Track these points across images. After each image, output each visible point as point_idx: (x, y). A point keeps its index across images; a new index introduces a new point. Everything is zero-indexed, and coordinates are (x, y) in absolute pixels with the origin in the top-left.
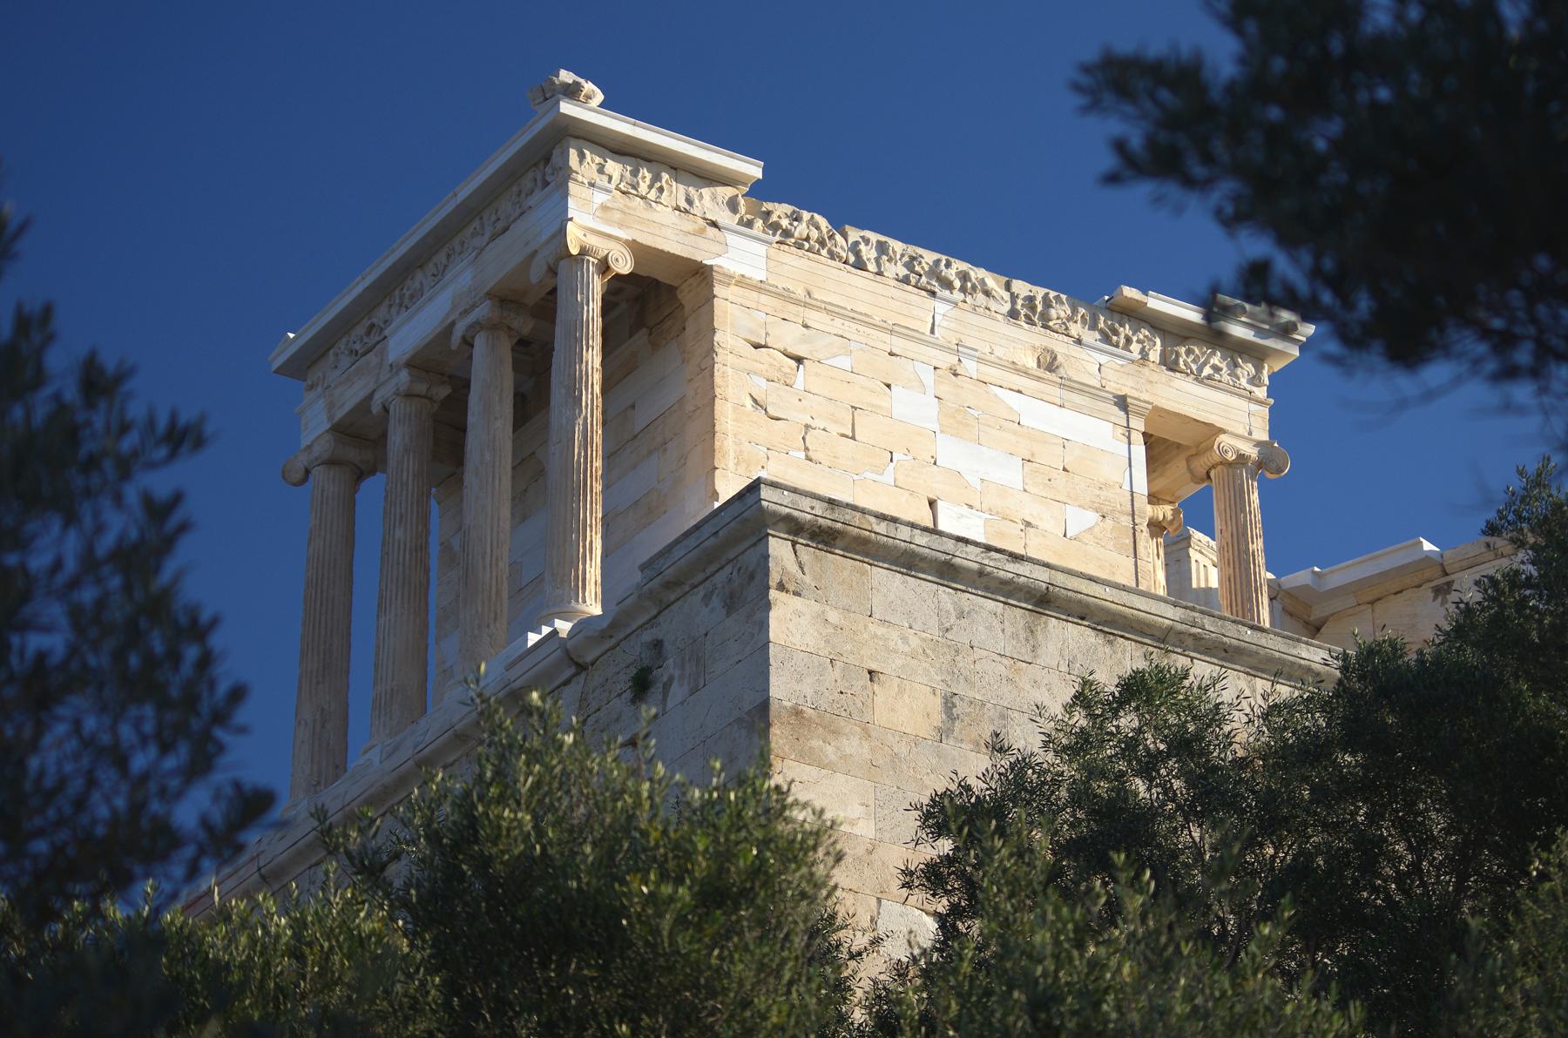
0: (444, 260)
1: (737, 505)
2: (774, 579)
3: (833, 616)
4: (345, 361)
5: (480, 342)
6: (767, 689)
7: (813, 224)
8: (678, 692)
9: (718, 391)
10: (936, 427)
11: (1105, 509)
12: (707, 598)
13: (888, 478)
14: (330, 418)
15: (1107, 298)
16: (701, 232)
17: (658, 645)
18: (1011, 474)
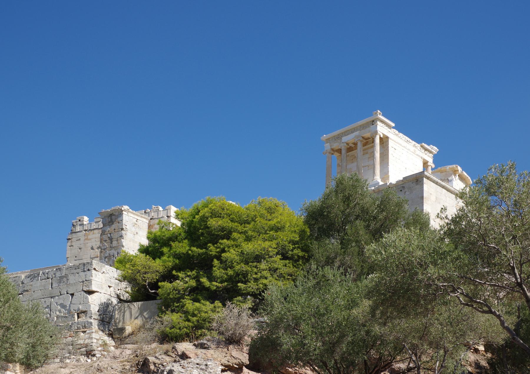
7: (397, 132)
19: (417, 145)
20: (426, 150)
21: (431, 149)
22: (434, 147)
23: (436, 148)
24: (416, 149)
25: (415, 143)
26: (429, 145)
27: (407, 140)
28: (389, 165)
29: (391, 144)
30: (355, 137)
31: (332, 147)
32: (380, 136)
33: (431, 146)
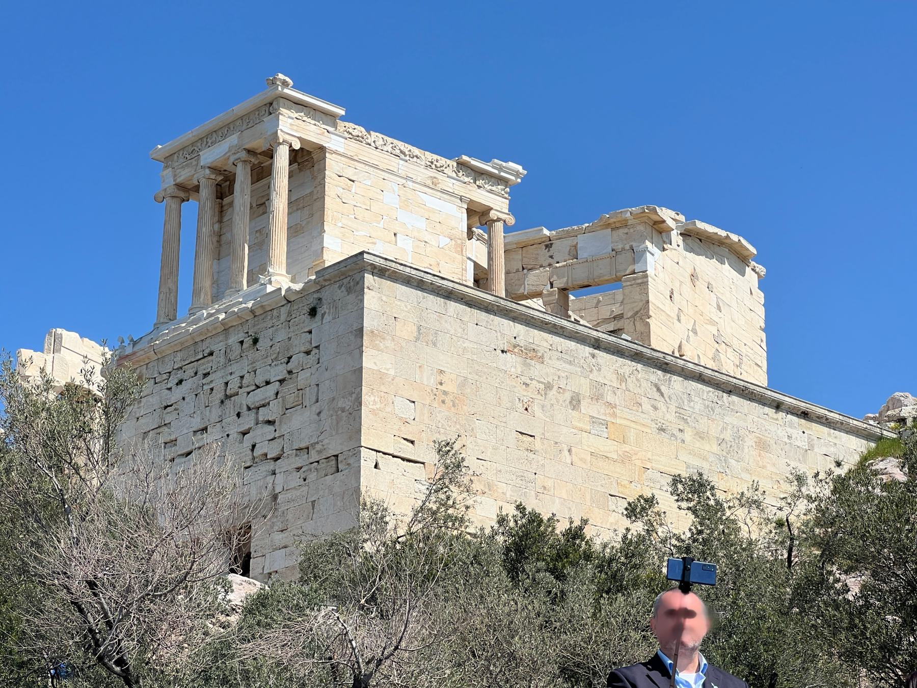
0: (226, 132)
1: (355, 259)
2: (366, 285)
3: (384, 298)
4: (182, 160)
5: (240, 166)
6: (362, 324)
7: (360, 130)
8: (327, 318)
9: (326, 193)
10: (398, 207)
11: (453, 237)
12: (340, 287)
13: (381, 225)
14: (174, 181)
15: (457, 159)
16: (322, 134)
17: (320, 299)
18: (422, 224)
19: (443, 161)
20: (478, 174)
21: (496, 172)
22: (511, 165)
23: (519, 168)
24: (439, 176)
25: (435, 157)
26: (487, 160)
27: (401, 152)
28: (325, 228)
29: (332, 165)
30: (229, 151)
31: (179, 180)
32: (291, 146)
33: (496, 161)
